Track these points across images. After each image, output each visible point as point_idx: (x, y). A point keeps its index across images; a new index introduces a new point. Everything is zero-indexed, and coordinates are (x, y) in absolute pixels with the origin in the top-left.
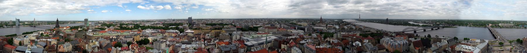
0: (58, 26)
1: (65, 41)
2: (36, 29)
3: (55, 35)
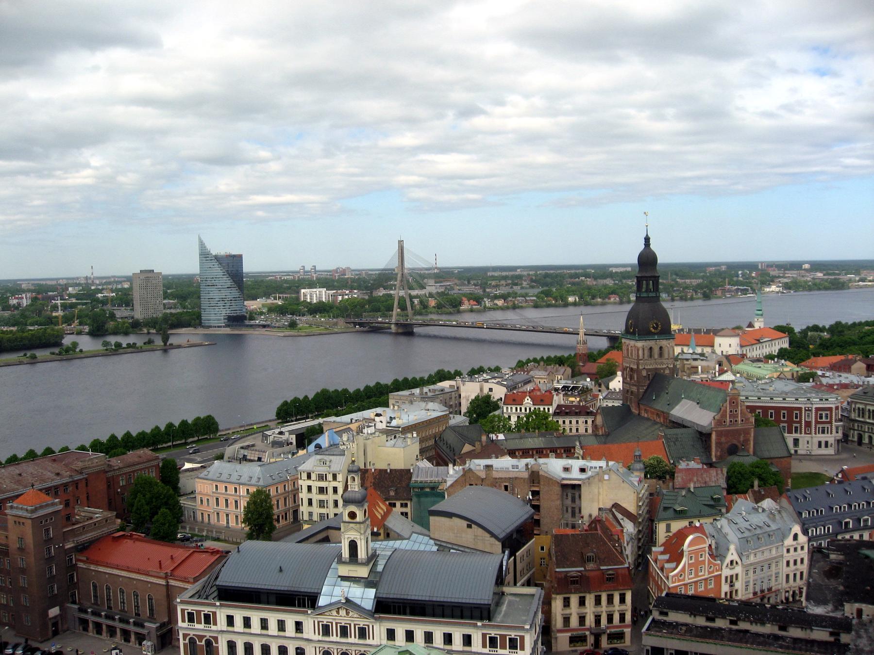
0: (649, 323)
1: (736, 485)
2: (424, 357)
3: (619, 422)
